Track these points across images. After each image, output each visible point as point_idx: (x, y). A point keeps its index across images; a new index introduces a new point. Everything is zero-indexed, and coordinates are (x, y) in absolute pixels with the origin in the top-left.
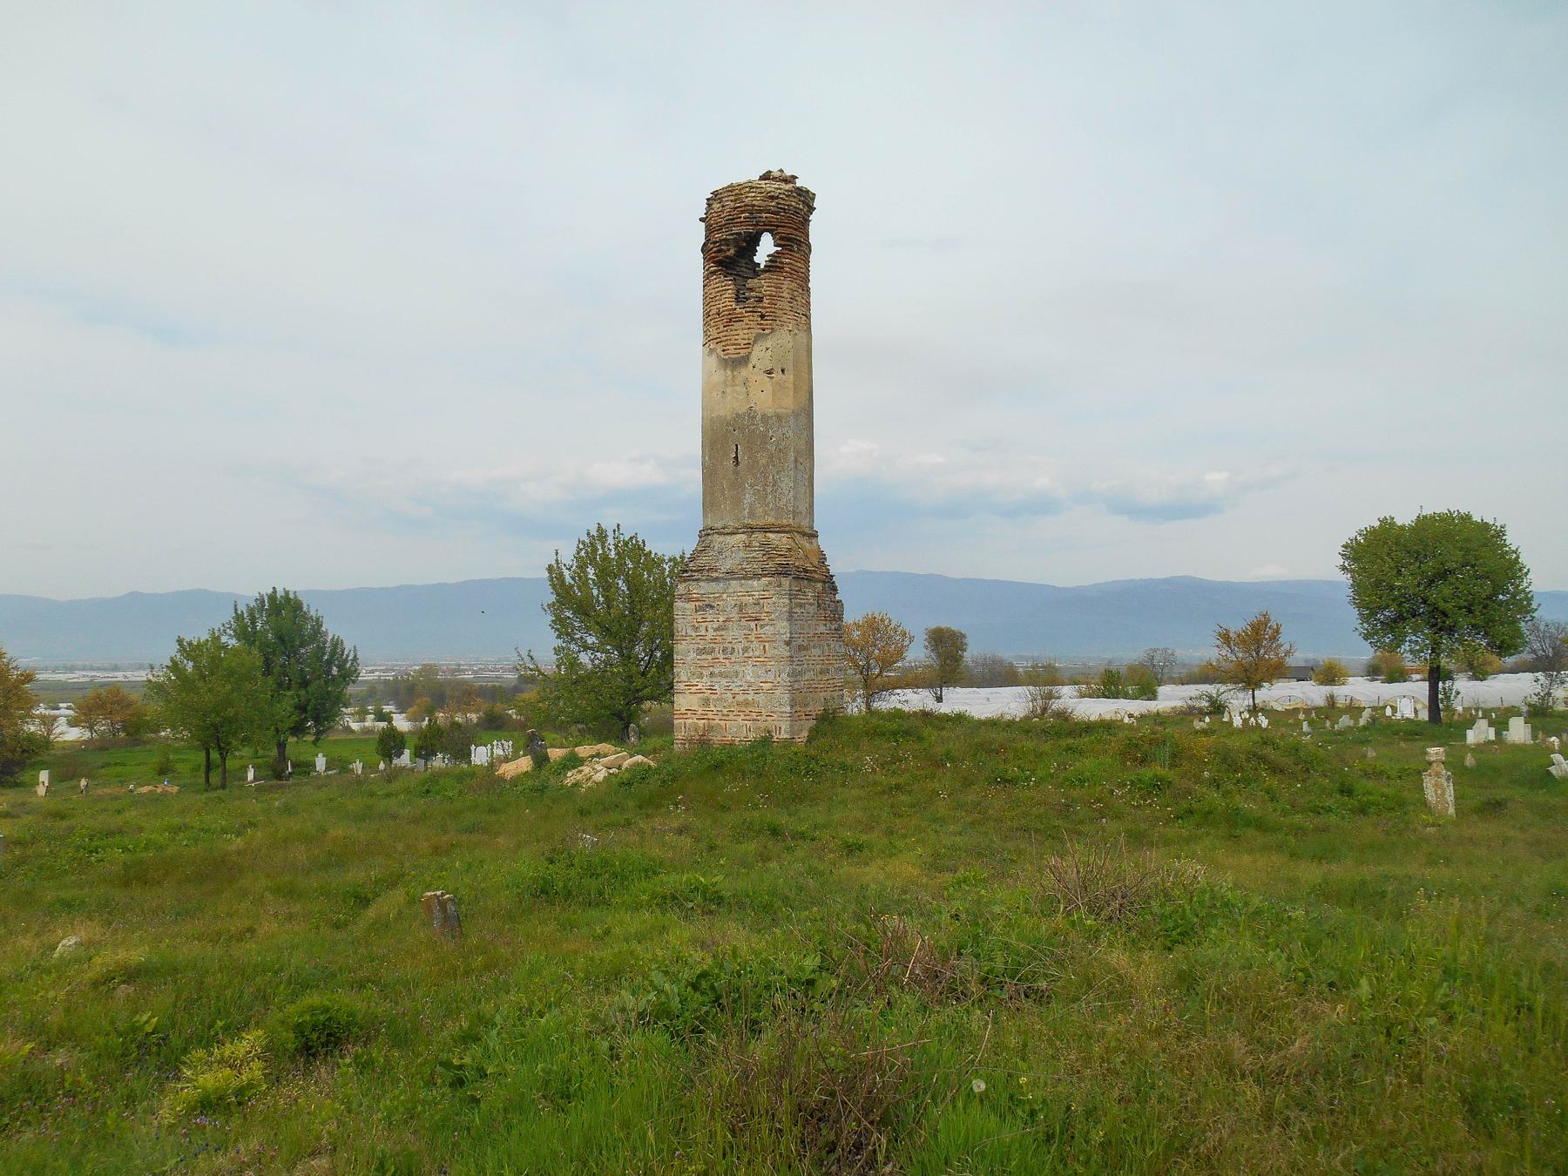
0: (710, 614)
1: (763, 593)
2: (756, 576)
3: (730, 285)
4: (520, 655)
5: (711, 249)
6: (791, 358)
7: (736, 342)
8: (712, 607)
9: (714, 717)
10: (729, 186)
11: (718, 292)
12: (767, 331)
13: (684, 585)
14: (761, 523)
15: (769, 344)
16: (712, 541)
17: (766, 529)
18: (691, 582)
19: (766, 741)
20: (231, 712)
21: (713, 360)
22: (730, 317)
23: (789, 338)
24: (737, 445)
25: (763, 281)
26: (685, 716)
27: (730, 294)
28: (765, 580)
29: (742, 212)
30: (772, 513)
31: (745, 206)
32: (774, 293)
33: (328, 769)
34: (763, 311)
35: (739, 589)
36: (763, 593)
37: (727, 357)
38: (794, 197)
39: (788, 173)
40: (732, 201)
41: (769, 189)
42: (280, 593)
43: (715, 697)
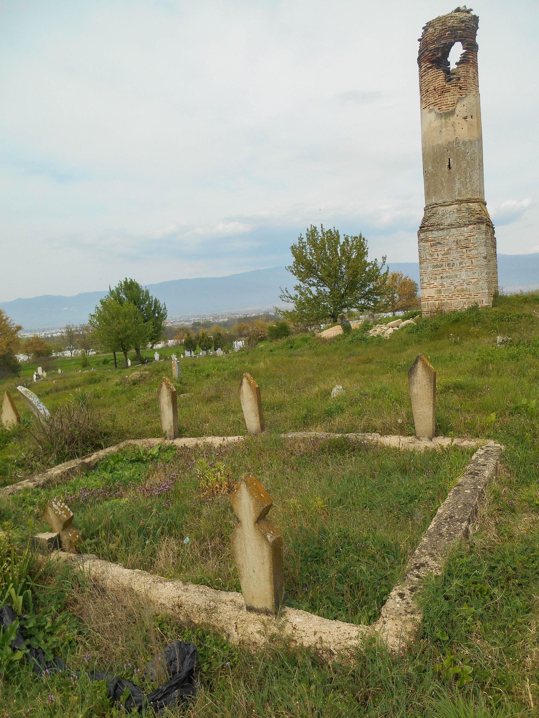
0: (439, 247)
1: (470, 233)
2: (466, 225)
3: (441, 73)
4: (282, 291)
5: (428, 55)
6: (475, 110)
7: (447, 103)
8: (440, 243)
9: (444, 299)
10: (437, 18)
11: (434, 77)
12: (463, 96)
13: (423, 234)
14: (464, 198)
15: (465, 102)
16: (437, 210)
17: (468, 201)
18: (427, 232)
19: (474, 308)
20: (129, 332)
21: (432, 116)
22: (442, 90)
23: (474, 99)
24: (449, 159)
25: (460, 69)
26: (428, 300)
27: (442, 77)
28: (471, 227)
29: (447, 31)
30: (470, 193)
31: (449, 27)
32: (466, 75)
33: (160, 359)
34: (461, 85)
35: (456, 233)
36: (470, 233)
37: (442, 112)
38: (472, 21)
39: (468, 8)
40: (440, 26)
41: (461, 17)
42: (129, 281)
43: (444, 288)
